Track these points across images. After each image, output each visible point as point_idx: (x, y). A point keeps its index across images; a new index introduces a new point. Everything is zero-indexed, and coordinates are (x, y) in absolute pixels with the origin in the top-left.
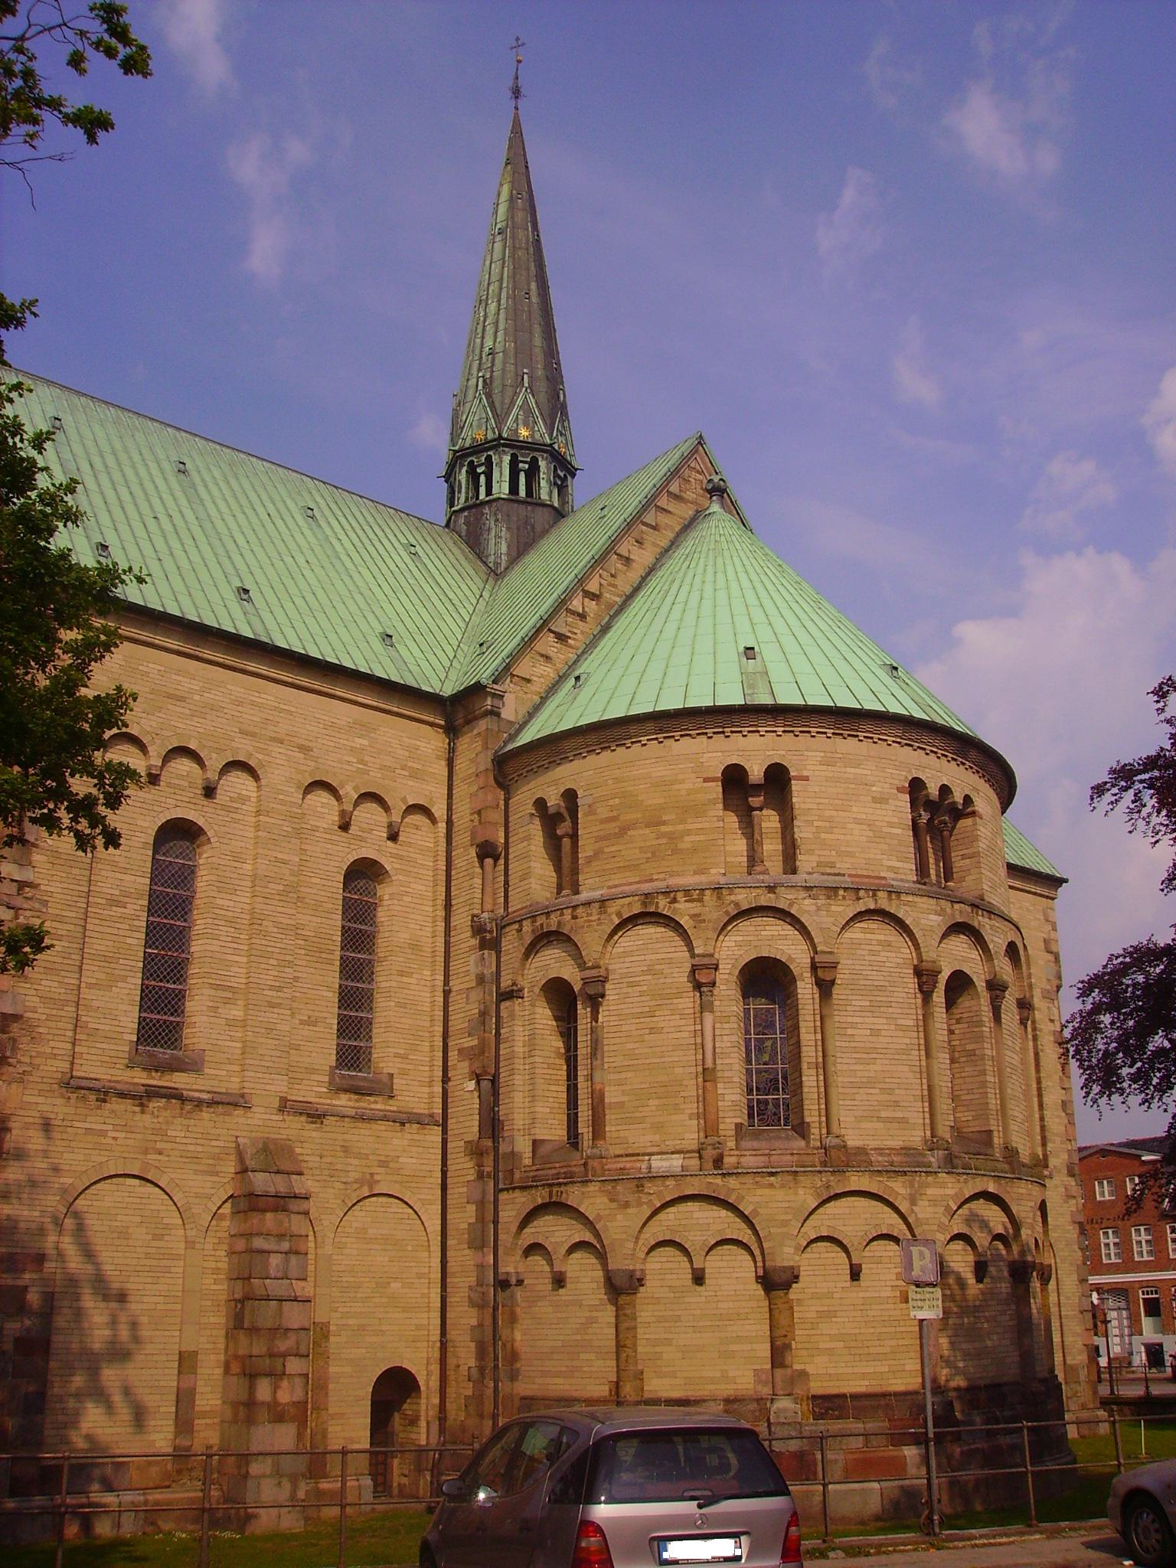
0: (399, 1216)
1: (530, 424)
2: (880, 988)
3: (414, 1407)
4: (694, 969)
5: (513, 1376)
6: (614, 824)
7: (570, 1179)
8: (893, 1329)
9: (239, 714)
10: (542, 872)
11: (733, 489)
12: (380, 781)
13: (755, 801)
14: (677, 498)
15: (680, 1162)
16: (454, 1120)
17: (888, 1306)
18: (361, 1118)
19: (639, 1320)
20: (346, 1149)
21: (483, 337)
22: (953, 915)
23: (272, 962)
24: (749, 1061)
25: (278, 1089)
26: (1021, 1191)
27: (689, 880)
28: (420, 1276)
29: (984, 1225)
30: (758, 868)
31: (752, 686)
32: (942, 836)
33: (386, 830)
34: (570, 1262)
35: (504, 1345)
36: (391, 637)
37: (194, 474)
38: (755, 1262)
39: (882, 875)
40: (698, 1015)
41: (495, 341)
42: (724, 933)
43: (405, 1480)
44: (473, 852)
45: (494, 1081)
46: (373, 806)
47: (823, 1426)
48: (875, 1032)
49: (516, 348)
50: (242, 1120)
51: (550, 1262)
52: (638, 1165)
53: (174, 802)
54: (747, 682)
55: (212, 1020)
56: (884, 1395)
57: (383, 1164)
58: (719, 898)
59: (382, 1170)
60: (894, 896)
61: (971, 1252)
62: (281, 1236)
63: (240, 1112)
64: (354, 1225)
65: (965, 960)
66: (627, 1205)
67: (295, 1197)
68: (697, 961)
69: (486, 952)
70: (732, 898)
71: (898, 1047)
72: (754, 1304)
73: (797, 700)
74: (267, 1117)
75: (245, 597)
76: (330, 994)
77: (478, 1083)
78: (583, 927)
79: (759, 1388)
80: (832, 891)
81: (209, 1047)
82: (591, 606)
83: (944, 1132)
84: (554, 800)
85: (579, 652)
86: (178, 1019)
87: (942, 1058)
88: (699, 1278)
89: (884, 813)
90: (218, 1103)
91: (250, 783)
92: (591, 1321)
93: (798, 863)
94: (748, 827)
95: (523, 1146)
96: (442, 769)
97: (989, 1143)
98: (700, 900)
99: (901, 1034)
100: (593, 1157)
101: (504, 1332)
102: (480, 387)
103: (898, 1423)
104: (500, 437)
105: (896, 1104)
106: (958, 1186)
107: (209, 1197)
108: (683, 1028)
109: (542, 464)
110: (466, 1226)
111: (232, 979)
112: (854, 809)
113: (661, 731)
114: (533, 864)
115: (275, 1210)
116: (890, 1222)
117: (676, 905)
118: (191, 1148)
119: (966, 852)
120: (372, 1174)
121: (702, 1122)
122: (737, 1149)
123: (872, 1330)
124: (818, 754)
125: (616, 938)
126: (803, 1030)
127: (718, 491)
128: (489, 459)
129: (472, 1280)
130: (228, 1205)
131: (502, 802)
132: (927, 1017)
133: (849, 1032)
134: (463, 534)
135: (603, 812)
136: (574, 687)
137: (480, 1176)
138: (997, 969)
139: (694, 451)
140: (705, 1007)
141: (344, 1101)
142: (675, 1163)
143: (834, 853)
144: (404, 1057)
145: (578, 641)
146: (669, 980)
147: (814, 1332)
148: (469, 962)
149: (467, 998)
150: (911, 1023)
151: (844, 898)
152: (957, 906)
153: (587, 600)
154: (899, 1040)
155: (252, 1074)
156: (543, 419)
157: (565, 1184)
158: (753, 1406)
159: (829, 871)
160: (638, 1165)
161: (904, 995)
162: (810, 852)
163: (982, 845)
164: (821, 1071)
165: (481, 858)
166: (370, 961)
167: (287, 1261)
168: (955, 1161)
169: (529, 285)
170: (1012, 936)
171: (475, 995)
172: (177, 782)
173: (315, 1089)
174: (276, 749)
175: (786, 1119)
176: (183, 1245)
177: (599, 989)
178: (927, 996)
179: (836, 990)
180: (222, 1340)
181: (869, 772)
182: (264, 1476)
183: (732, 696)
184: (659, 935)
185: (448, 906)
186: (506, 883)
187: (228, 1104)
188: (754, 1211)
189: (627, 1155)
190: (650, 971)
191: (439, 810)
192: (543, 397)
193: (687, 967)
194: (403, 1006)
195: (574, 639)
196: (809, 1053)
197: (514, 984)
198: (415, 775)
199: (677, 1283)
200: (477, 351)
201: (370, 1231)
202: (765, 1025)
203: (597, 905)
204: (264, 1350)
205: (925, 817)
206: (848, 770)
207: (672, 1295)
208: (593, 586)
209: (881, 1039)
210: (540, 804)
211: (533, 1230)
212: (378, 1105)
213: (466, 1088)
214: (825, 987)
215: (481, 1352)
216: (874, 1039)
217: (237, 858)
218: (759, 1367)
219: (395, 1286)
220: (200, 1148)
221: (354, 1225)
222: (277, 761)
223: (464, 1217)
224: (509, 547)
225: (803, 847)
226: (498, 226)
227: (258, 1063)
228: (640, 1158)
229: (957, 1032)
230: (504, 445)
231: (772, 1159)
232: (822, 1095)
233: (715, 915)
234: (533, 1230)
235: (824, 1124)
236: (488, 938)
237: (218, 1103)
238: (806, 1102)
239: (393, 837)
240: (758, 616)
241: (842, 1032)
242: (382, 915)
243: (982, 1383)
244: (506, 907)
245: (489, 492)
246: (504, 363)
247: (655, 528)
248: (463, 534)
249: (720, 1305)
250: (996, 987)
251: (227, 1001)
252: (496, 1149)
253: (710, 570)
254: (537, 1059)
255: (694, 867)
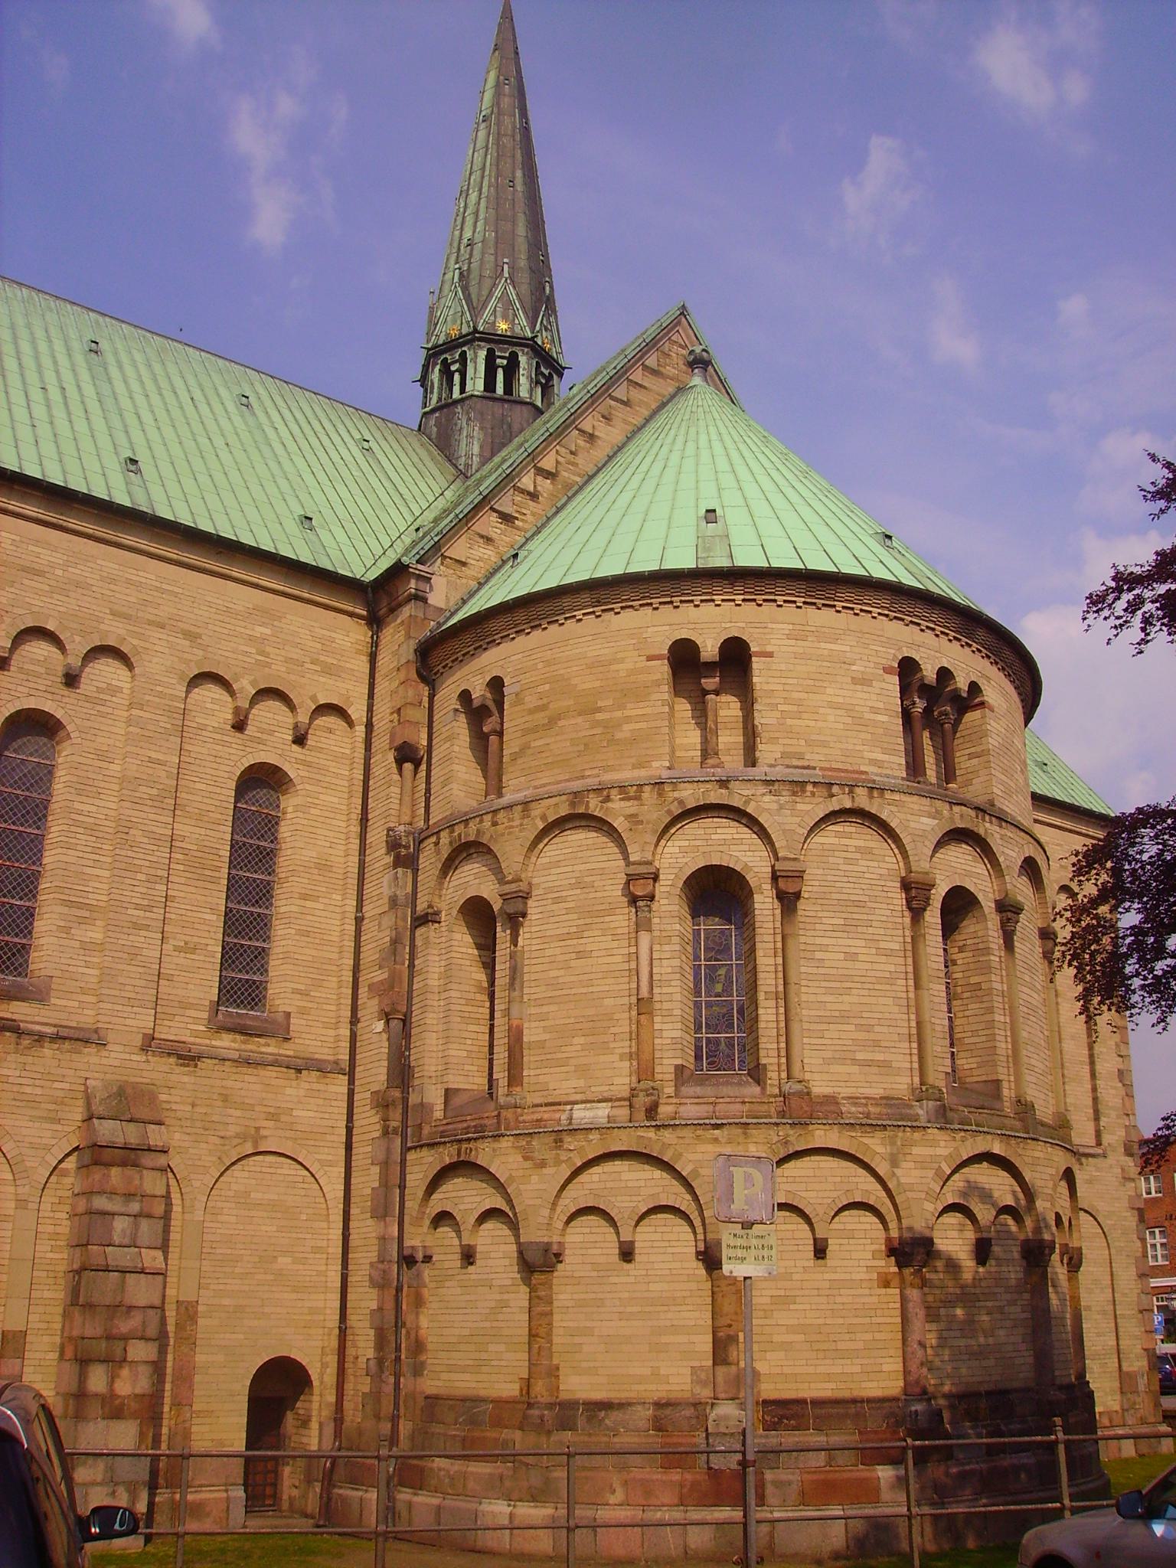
0: (290, 1178)
1: (509, 316)
2: (858, 904)
3: (306, 1405)
4: (628, 883)
5: (418, 1370)
6: (543, 714)
7: (480, 1133)
8: (868, 1320)
9: (112, 594)
10: (467, 777)
11: (719, 362)
12: (285, 675)
13: (710, 682)
14: (655, 372)
15: (607, 1112)
16: (362, 1068)
17: (860, 1291)
18: (248, 1062)
19: (556, 1304)
20: (225, 1098)
21: (462, 229)
22: (952, 819)
23: (140, 876)
24: (697, 992)
25: (141, 1024)
26: (1037, 1154)
27: (626, 775)
28: (316, 1250)
29: (986, 1196)
30: (710, 761)
31: (708, 550)
32: (943, 731)
33: (291, 732)
34: (481, 1233)
35: (408, 1332)
36: (311, 519)
37: (110, 359)
38: (695, 1233)
39: (863, 768)
40: (633, 935)
41: (474, 232)
42: (668, 835)
43: (295, 1492)
44: (391, 756)
45: (406, 1022)
46: (276, 705)
47: (774, 1439)
48: (852, 957)
49: (497, 237)
50: (94, 1060)
51: (458, 1232)
52: (557, 1116)
53: (26, 690)
54: (702, 544)
55: (62, 941)
56: (854, 1401)
57: (273, 1117)
58: (660, 795)
59: (271, 1124)
60: (876, 793)
61: (971, 1227)
62: (129, 1196)
63: (93, 1049)
64: (234, 1187)
65: (969, 874)
66: (542, 1164)
67: (149, 1150)
68: (632, 870)
69: (400, 870)
70: (676, 794)
71: (879, 974)
72: (694, 1286)
73: (760, 562)
74: (127, 1057)
75: (133, 468)
76: (214, 917)
77: (387, 1022)
78: (503, 835)
79: (698, 1390)
80: (798, 787)
81: (58, 973)
82: (544, 485)
83: (937, 1077)
84: (479, 692)
85: (528, 535)
86: (24, 941)
87: (937, 990)
88: (627, 1254)
89: (866, 695)
90: (65, 1038)
91: (123, 672)
92: (503, 1305)
93: (758, 754)
94: (702, 715)
95: (434, 1097)
96: (362, 665)
97: (997, 1095)
98: (637, 798)
99: (883, 959)
100: (507, 1107)
101: (409, 1319)
102: (456, 279)
103: (872, 1436)
104: (476, 331)
105: (876, 1044)
106: (954, 1144)
107: (48, 1148)
108: (615, 952)
109: (523, 360)
110: (369, 1191)
111: (91, 896)
112: (829, 691)
113: (599, 603)
114: (456, 767)
115: (124, 1164)
116: (865, 1187)
117: (610, 805)
118: (28, 1090)
119: (973, 750)
120: (258, 1129)
121: (635, 1063)
122: (676, 1096)
123: (841, 1321)
124: (785, 626)
125: (541, 846)
126: (759, 953)
127: (700, 363)
128: (463, 355)
129: (373, 1256)
130: (73, 1158)
131: (426, 700)
132: (916, 939)
133: (818, 955)
134: (434, 436)
135: (531, 701)
136: (512, 567)
137: (386, 1132)
138: (1009, 886)
139: (675, 323)
140: (642, 925)
141: (227, 1043)
142: (601, 1113)
143: (802, 742)
144: (304, 994)
145: (527, 522)
146: (599, 895)
147: (767, 1321)
148: (383, 882)
149: (380, 924)
150: (897, 946)
151: (813, 794)
152: (956, 809)
153: (539, 479)
154: (882, 967)
155: (109, 1006)
156: (525, 313)
157: (475, 1139)
158: (689, 1412)
159: (795, 762)
160: (557, 1116)
161: (888, 913)
162: (773, 740)
163: (993, 742)
164: (782, 1003)
165: (400, 762)
166: (268, 882)
167: (136, 1226)
168: (950, 1114)
169: (513, 173)
170: (1031, 850)
171: (388, 921)
172: (32, 667)
173: (189, 1026)
174: (155, 634)
175: (741, 1062)
176: (13, 1205)
177: (520, 907)
178: (916, 913)
179: (801, 905)
180: (59, 1319)
181: (848, 649)
182: (94, 1484)
183: (685, 560)
184: (590, 842)
185: (364, 820)
186: (428, 791)
187: (77, 1040)
188: (695, 1171)
189: (547, 1105)
190: (579, 884)
191: (358, 712)
192: (525, 289)
193: (622, 878)
194: (307, 934)
195: (523, 520)
196: (768, 981)
197: (430, 906)
198: (328, 670)
199: (602, 1259)
200: (455, 244)
201: (253, 1195)
202: (718, 949)
203: (519, 808)
204: (99, 1331)
205: (920, 705)
206: (823, 645)
207: (595, 1274)
208: (548, 463)
209: (858, 965)
210: (465, 696)
211: (441, 1196)
212: (270, 1048)
213: (374, 1027)
214: (788, 901)
215: (380, 1343)
216: (849, 964)
217: (102, 756)
218: (696, 1364)
219: (284, 1261)
220: (39, 1091)
221: (234, 1187)
222: (156, 648)
223: (367, 1180)
224: (481, 447)
225: (764, 735)
226: (483, 113)
227: (117, 993)
228: (561, 1107)
229: (959, 962)
230: (480, 339)
231: (717, 1108)
232: (783, 1031)
233: (655, 816)
234: (441, 1196)
235: (784, 1067)
236: (404, 857)
237: (65, 1038)
238: (762, 1040)
239: (300, 740)
240: (727, 480)
241: (808, 955)
242: (284, 830)
243: (983, 1388)
244: (427, 819)
245: (463, 390)
246: (483, 253)
247: (626, 403)
248: (434, 436)
249: (652, 1287)
250: (1008, 909)
251: (82, 921)
252: (405, 1100)
253: (680, 439)
254: (453, 994)
255: (633, 760)
